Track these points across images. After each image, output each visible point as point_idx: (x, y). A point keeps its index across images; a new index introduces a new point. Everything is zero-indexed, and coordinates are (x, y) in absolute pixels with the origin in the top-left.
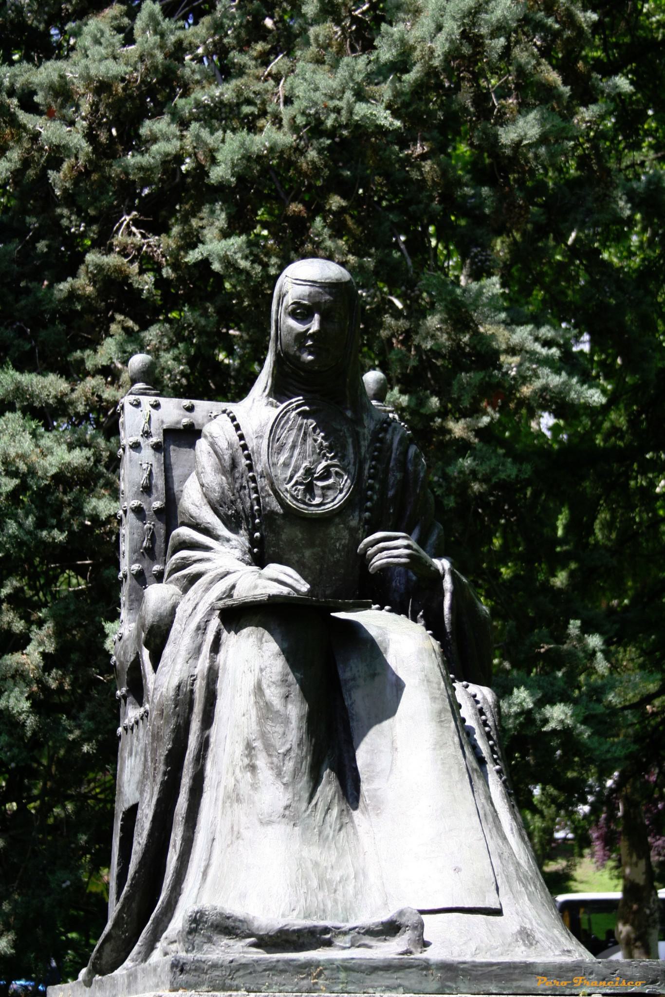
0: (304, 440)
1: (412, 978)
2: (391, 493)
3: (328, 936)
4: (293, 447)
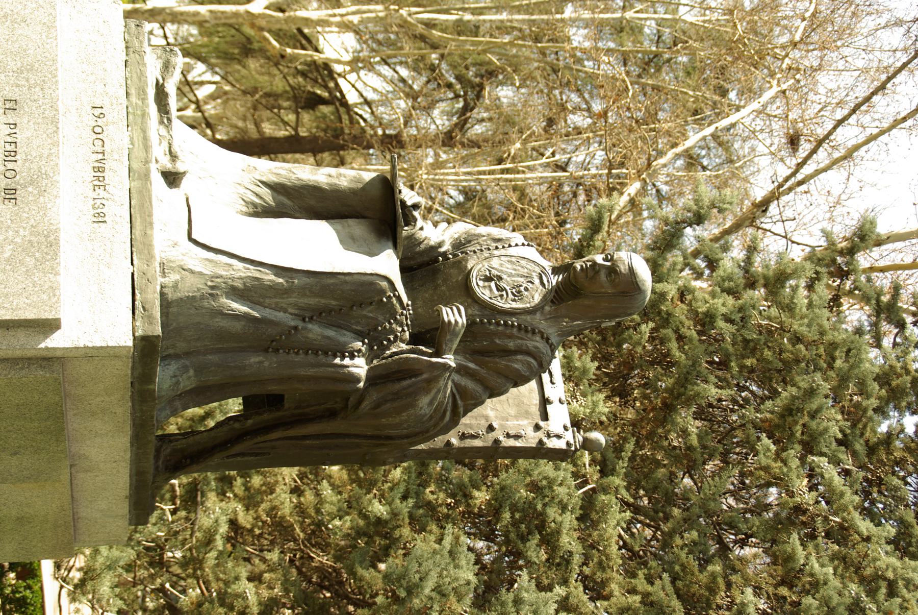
0: (522, 276)
1: (139, 153)
2: (497, 341)
3: (165, 121)
4: (515, 270)
